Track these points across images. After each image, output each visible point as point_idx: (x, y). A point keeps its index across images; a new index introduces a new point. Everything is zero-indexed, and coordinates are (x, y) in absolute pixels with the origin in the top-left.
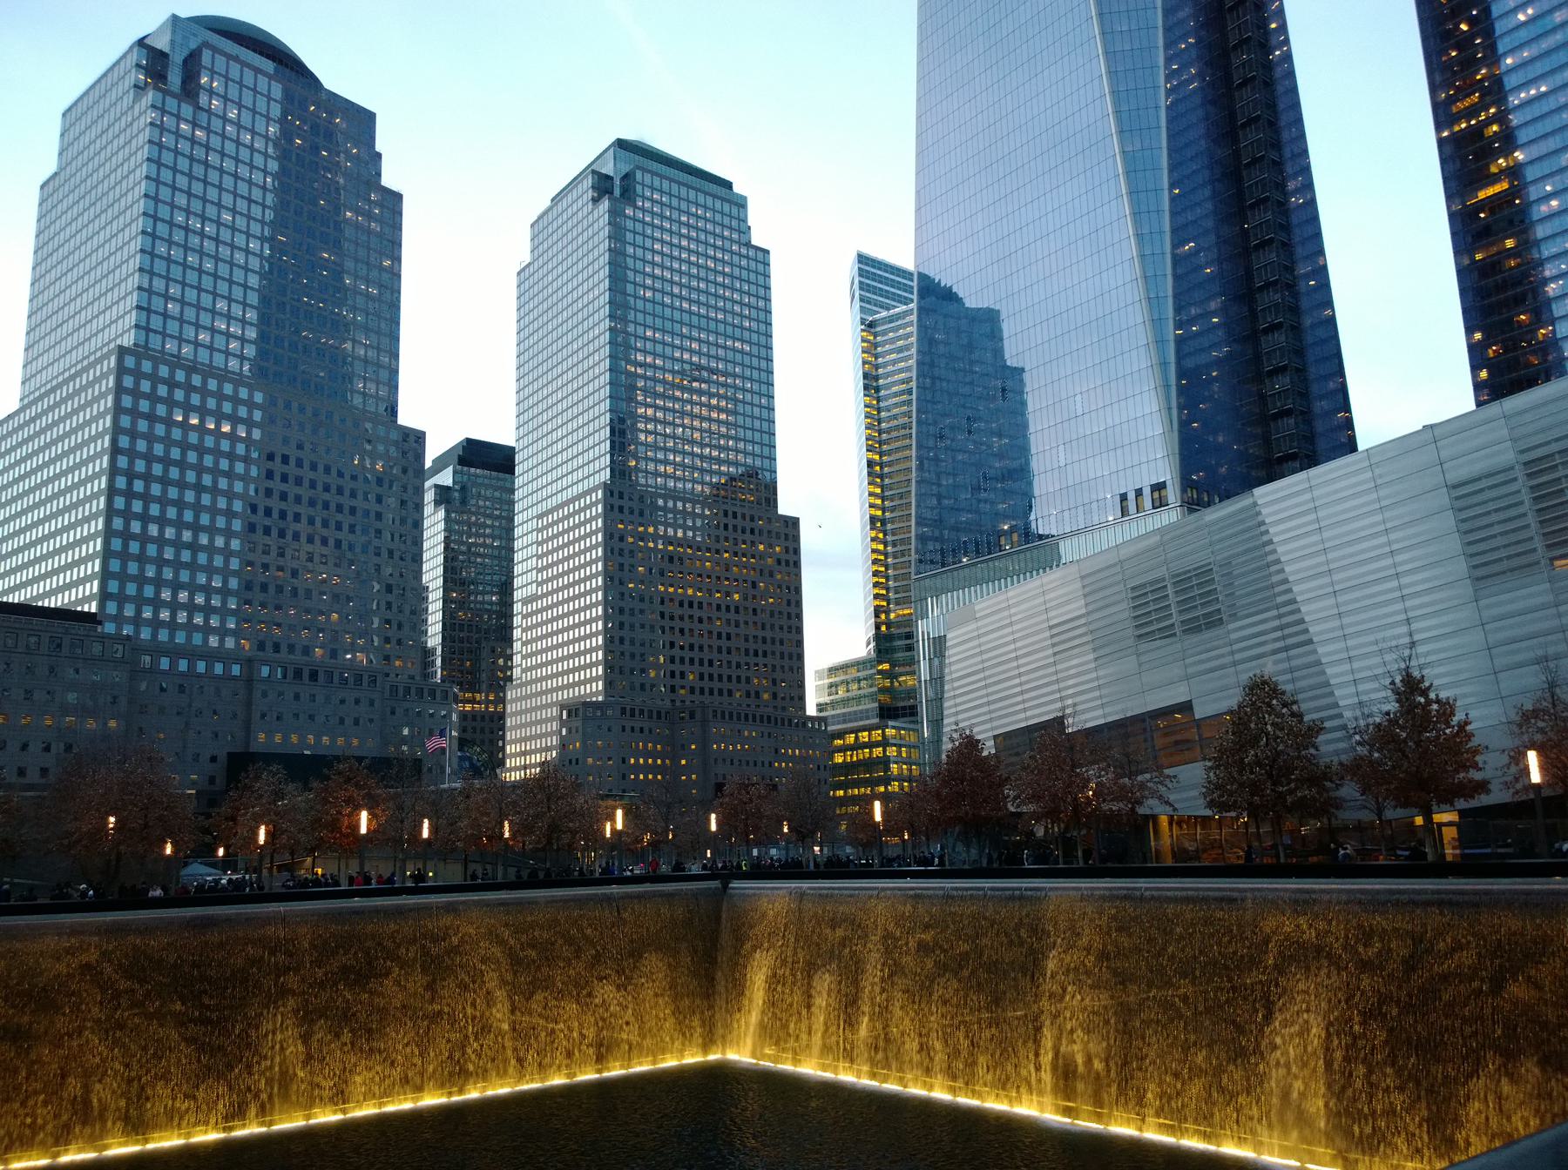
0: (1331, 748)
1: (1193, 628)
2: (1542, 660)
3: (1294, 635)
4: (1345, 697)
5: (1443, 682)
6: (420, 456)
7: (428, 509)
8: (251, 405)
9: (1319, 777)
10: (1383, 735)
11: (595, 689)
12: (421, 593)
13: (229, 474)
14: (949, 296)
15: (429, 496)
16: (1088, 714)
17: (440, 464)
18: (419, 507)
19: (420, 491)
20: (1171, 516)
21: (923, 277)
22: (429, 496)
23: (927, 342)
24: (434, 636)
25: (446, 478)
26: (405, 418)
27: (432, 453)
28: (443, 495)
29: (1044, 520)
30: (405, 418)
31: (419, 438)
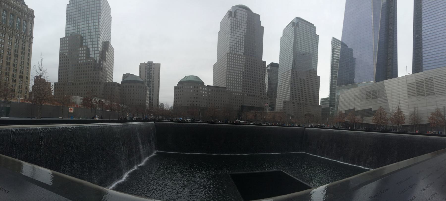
0: (388, 116)
1: (374, 98)
2: (414, 108)
3: (386, 101)
4: (391, 110)
5: (403, 109)
6: (265, 65)
7: (266, 73)
8: (243, 59)
9: (386, 120)
10: (395, 116)
11: (288, 99)
12: (265, 84)
13: (241, 68)
14: (346, 46)
15: (266, 71)
16: (358, 109)
17: (268, 66)
18: (265, 72)
19: (265, 70)
20: (373, 81)
21: (342, 42)
22: (266, 71)
23: (342, 52)
24: (266, 91)
25: (269, 68)
26: (263, 60)
27: (267, 64)
28: (268, 71)
29: (356, 80)
30: (263, 60)
31: (265, 62)
